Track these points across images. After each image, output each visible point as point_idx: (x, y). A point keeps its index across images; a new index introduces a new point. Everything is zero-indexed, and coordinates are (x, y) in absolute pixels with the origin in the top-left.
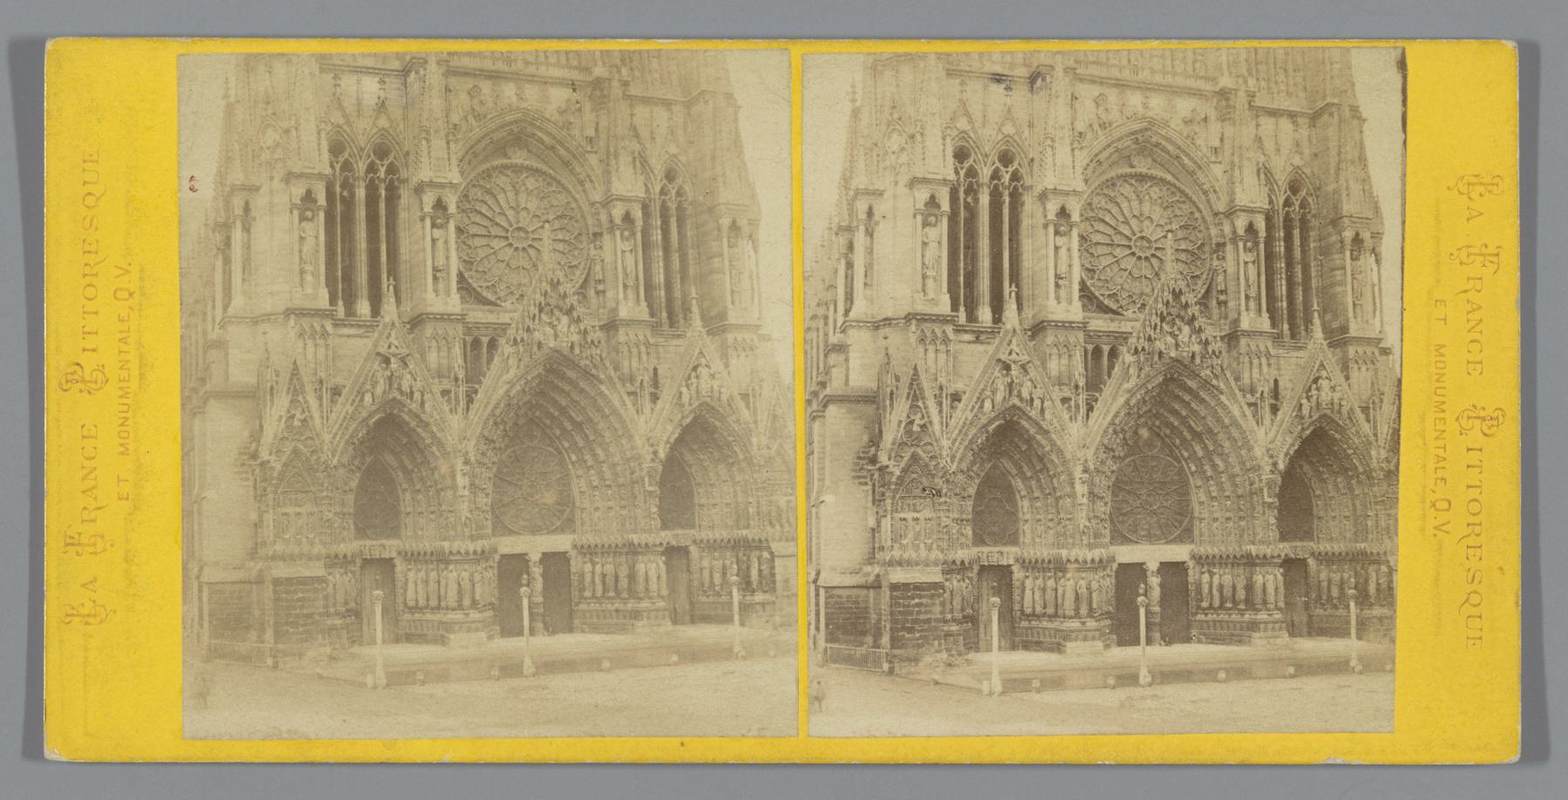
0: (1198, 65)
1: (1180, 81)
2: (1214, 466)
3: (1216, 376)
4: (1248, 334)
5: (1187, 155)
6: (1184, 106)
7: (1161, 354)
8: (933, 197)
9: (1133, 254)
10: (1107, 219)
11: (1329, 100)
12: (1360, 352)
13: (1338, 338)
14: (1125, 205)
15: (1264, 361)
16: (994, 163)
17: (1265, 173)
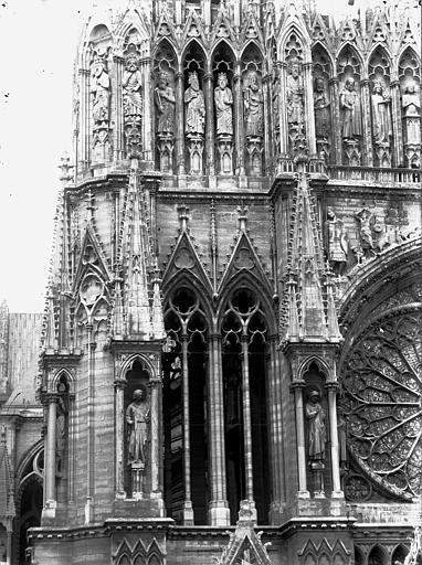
8: (138, 364)
16: (227, 308)
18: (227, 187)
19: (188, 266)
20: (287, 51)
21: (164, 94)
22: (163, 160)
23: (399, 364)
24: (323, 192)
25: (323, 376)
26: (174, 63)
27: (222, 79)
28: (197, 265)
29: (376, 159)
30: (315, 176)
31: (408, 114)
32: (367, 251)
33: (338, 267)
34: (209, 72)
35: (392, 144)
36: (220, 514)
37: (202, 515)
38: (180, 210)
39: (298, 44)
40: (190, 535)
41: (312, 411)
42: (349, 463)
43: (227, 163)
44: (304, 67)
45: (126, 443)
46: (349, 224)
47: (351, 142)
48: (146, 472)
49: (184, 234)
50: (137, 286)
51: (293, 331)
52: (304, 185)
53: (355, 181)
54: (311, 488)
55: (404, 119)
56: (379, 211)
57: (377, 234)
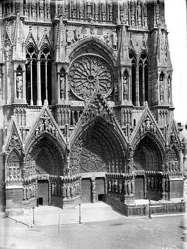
0: (111, 17)
1: (105, 24)
2: (112, 148)
3: (111, 121)
4: (124, 107)
5: (106, 49)
6: (105, 32)
7: (94, 115)
8: (19, 66)
9: (88, 81)
10: (79, 70)
11: (155, 28)
12: (162, 111)
13: (154, 107)
14: (85, 66)
15: (129, 115)
17: (132, 54)
18: (42, 21)
19: (32, 42)
23: (83, 69)
25: (65, 71)
28: (34, 42)
30: (64, 20)
32: (76, 40)
33: (69, 44)
36: (39, 103)
37: (35, 103)
38: (30, 27)
40: (32, 108)
41: (61, 79)
42: (70, 92)
43: (42, 15)
45: (17, 85)
48: (22, 92)
50: (19, 46)
51: (57, 60)
52: (61, 22)
53: (75, 21)
54: (61, 97)
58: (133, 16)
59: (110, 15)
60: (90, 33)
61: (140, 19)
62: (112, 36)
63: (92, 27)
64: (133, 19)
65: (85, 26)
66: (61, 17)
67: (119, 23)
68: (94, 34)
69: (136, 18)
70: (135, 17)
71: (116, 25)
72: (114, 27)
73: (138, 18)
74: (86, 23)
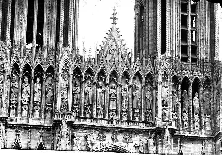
1: (137, 126)
18: (36, 123)
20: (63, 69)
21: (14, 84)
22: (12, 111)
24: (71, 125)
26: (19, 73)
27: (38, 80)
29: (97, 114)
30: (69, 120)
31: (111, 97)
34: (33, 76)
35: (104, 109)
38: (17, 131)
39: (68, 67)
43: (37, 113)
44: (69, 76)
46: (82, 139)
47: (88, 107)
49: (17, 141)
52: (64, 124)
53: (88, 122)
55: (110, 99)
56: (95, 135)
57: (93, 144)
58: (186, 114)
59: (147, 113)
60: (111, 141)
61: (197, 119)
62: (148, 145)
63: (114, 132)
64: (186, 118)
65: (102, 130)
66: (65, 117)
67: (160, 123)
68: (118, 141)
69: (192, 116)
70: (189, 115)
71: (154, 128)
72: (152, 131)
73: (194, 117)
74: (107, 124)
